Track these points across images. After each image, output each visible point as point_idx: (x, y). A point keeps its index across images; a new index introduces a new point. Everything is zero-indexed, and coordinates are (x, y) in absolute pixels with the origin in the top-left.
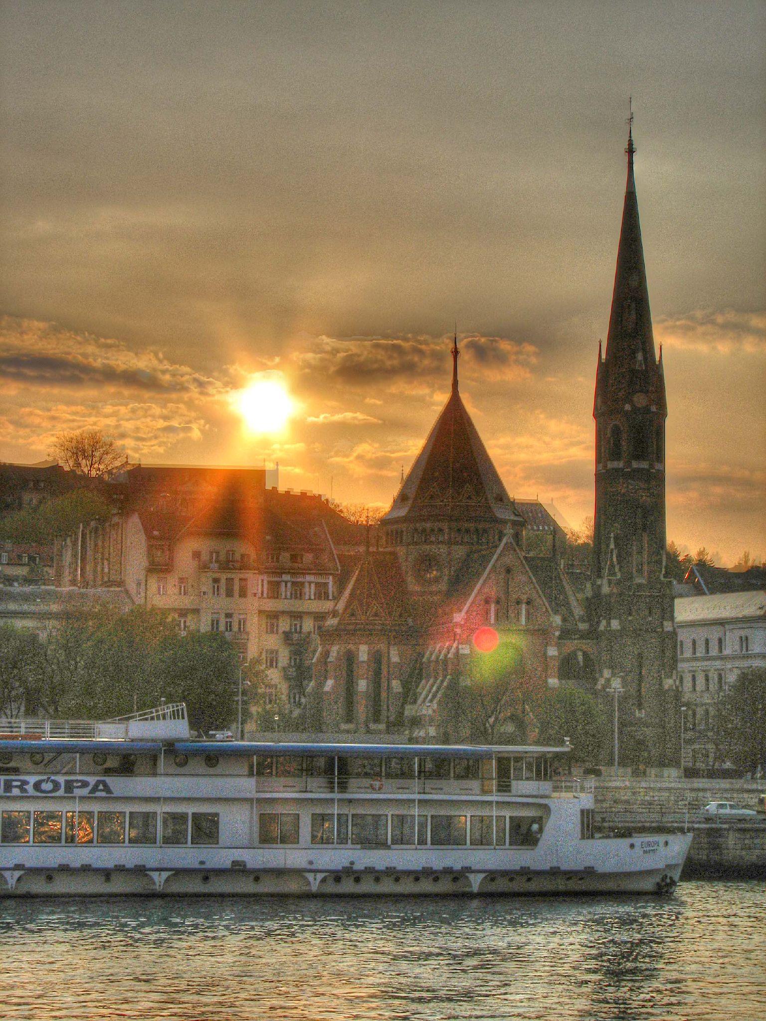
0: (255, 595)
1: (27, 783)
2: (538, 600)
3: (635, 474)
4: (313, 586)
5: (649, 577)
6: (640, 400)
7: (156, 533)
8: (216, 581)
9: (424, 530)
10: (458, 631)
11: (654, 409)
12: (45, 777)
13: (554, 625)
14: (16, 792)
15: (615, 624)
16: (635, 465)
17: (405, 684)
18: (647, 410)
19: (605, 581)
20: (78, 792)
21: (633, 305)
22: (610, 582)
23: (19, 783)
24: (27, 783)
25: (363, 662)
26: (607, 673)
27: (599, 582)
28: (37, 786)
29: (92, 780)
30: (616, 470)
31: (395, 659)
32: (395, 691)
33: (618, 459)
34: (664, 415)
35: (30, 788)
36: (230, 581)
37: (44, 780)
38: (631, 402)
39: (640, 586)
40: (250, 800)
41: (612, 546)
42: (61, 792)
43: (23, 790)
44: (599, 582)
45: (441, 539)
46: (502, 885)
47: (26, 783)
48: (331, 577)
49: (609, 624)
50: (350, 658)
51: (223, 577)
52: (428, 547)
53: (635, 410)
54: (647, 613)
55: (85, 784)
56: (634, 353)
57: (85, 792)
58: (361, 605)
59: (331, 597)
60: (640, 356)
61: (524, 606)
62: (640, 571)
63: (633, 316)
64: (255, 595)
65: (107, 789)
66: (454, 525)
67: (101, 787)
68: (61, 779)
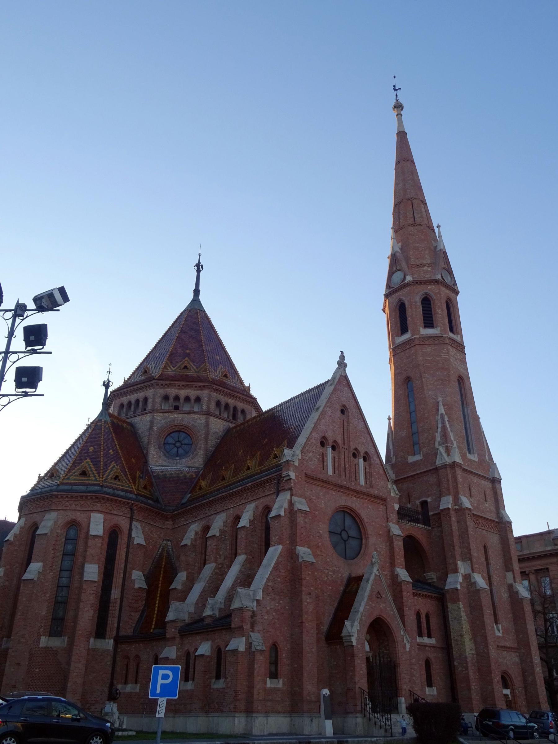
2: (375, 458)
9: (177, 398)
10: (292, 475)
17: (150, 578)
25: (95, 537)
26: (463, 567)
31: (139, 538)
32: (137, 586)
45: (196, 409)
52: (181, 416)
58: (96, 463)
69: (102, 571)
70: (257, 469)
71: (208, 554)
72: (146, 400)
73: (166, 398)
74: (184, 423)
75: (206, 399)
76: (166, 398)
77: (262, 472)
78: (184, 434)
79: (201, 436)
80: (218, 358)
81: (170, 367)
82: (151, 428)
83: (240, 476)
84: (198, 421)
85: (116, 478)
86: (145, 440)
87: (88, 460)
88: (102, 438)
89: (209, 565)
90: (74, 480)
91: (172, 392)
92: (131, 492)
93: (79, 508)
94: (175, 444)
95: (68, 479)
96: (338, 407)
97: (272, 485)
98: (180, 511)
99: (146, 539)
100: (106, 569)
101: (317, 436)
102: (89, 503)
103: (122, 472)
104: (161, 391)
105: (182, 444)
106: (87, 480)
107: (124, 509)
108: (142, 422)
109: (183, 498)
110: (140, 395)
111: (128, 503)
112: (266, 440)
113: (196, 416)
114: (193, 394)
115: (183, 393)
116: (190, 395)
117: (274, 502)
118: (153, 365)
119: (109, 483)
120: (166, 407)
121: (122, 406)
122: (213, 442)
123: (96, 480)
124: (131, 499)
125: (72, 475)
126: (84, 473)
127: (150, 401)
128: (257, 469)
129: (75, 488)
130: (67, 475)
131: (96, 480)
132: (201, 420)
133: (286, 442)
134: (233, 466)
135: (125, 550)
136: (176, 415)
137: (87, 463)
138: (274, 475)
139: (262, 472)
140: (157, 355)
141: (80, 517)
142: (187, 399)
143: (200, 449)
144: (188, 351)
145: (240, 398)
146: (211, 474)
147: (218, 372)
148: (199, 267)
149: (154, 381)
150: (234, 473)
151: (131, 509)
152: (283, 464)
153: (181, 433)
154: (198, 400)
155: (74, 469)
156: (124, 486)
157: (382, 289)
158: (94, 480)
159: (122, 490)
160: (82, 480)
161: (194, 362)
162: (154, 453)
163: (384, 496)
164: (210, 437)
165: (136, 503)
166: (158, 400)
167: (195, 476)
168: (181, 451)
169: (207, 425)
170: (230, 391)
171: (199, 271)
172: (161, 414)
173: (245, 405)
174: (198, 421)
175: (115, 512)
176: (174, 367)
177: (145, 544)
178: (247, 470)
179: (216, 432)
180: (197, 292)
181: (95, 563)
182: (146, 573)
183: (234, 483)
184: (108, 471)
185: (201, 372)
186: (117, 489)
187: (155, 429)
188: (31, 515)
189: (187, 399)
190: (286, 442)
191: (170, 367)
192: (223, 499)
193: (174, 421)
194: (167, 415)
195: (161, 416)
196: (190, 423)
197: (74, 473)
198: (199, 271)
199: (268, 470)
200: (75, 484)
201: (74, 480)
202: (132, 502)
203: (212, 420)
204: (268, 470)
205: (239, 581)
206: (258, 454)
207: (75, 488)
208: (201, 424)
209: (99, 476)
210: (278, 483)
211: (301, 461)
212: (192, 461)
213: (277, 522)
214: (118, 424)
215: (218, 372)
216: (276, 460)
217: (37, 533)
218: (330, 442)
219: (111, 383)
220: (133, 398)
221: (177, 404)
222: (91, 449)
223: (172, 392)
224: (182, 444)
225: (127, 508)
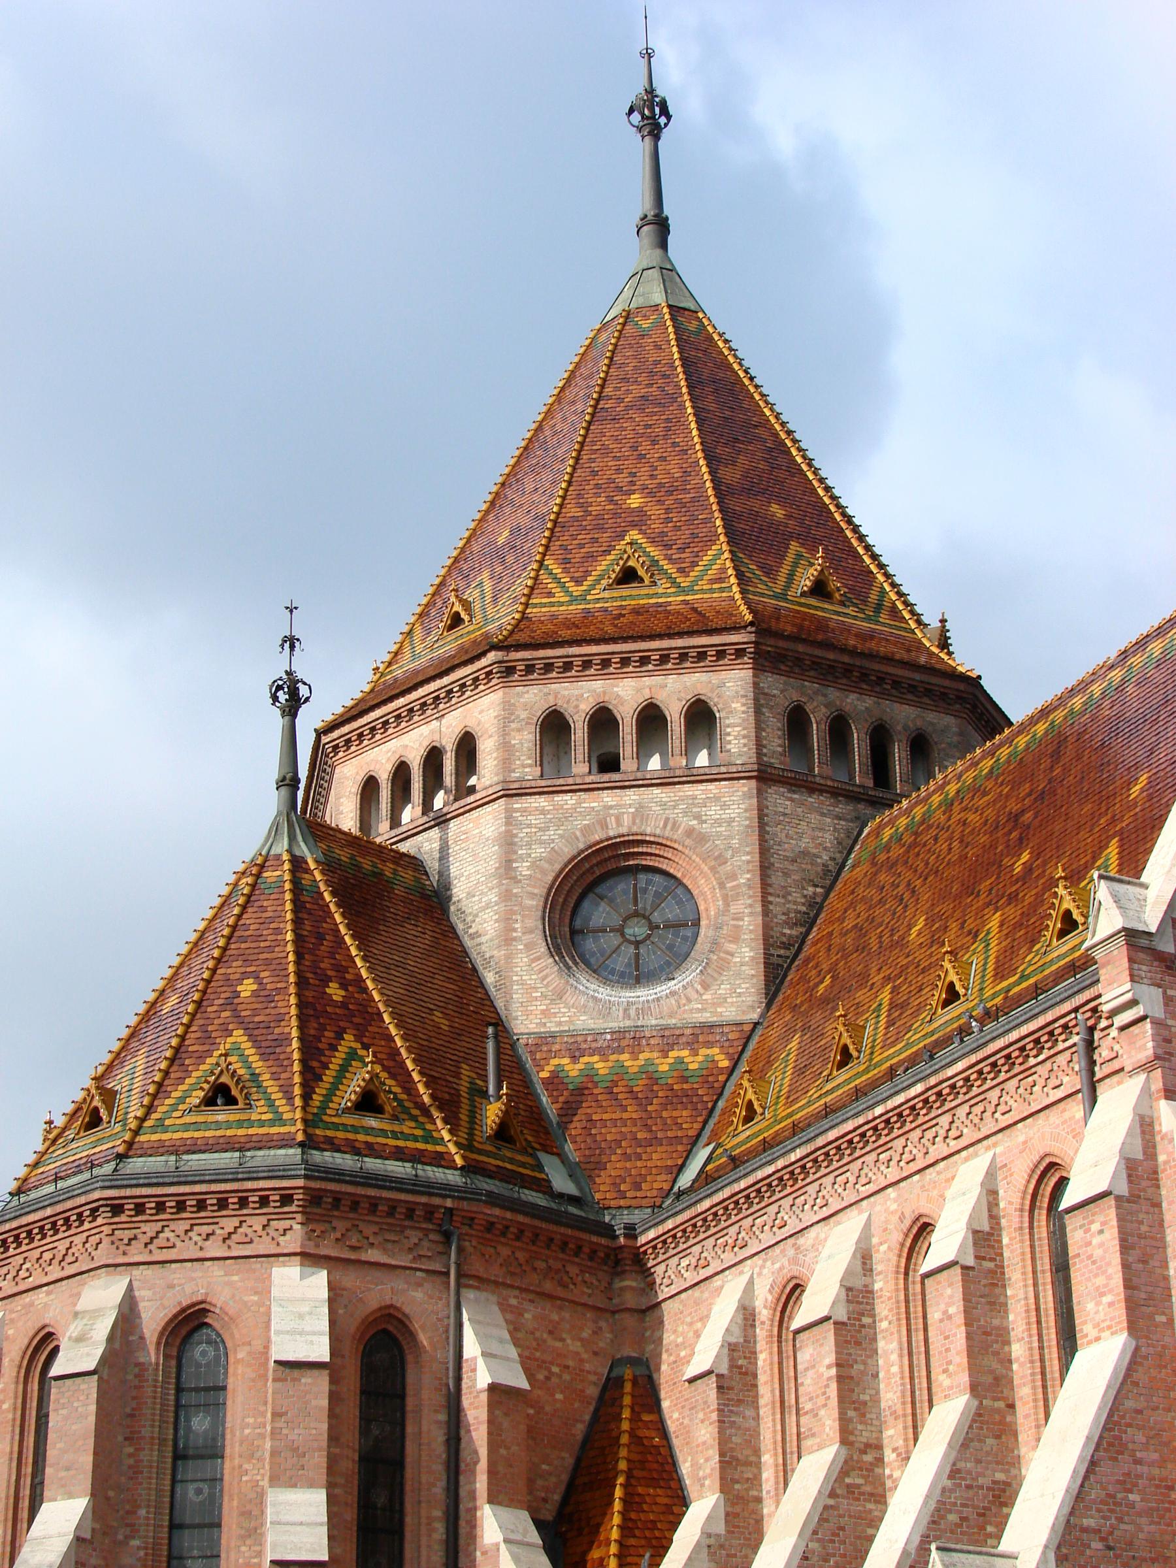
9: (603, 721)
52: (631, 797)
58: (270, 1050)
69: (350, 1515)
70: (988, 993)
71: (806, 1406)
72: (467, 746)
74: (651, 828)
75: (737, 706)
77: (1013, 1002)
78: (657, 878)
79: (733, 877)
80: (777, 511)
81: (563, 586)
83: (917, 1038)
84: (713, 811)
87: (239, 1036)
88: (289, 936)
89: (811, 1457)
90: (186, 1127)
91: (578, 697)
93: (214, 1249)
94: (621, 931)
95: (160, 1126)
97: (1062, 1060)
98: (670, 1224)
99: (529, 1366)
100: (365, 1505)
102: (257, 1223)
103: (392, 1076)
104: (535, 698)
105: (653, 927)
106: (240, 1124)
107: (414, 1236)
109: (681, 1168)
111: (430, 1212)
112: (1025, 857)
113: (698, 790)
114: (673, 690)
115: (626, 693)
116: (661, 699)
117: (1078, 1136)
118: (488, 586)
119: (336, 1127)
121: (370, 786)
123: (279, 1120)
124: (446, 1190)
125: (174, 1108)
127: (487, 750)
128: (988, 993)
129: (195, 1161)
130: (150, 1109)
131: (279, 1120)
132: (724, 806)
133: (1112, 851)
134: (885, 996)
135: (442, 1417)
136: (608, 798)
137: (237, 1048)
138: (1067, 1006)
139: (1013, 1002)
140: (501, 540)
142: (651, 719)
143: (736, 939)
144: (635, 501)
145: (896, 684)
146: (794, 1044)
147: (782, 579)
149: (492, 656)
150: (890, 1023)
152: (1098, 955)
153: (642, 877)
155: (181, 1080)
156: (407, 1137)
158: (272, 1123)
159: (399, 1155)
160: (218, 1125)
161: (668, 547)
162: (531, 979)
164: (777, 880)
165: (465, 1205)
166: (526, 739)
167: (725, 1064)
170: (846, 659)
171: (653, 130)
172: (541, 802)
173: (931, 716)
174: (713, 811)
175: (373, 1255)
176: (578, 582)
177: (524, 1384)
178: (946, 1003)
179: (805, 853)
180: (659, 226)
181: (311, 1485)
182: (548, 1515)
183: (891, 1073)
184: (329, 1077)
185: (703, 584)
186: (372, 1150)
187: (523, 868)
188: (27, 1298)
189: (651, 719)
190: (1112, 851)
191: (563, 586)
192: (848, 1146)
193: (604, 825)
194: (569, 800)
195: (543, 812)
196: (675, 826)
197: (182, 1100)
198: (653, 130)
199: (1037, 990)
200: (194, 1148)
201: (186, 1127)
202: (449, 1203)
204: (1037, 990)
205: (952, 1518)
206: (994, 923)
207: (195, 1161)
208: (730, 821)
209: (290, 1099)
210: (1090, 1046)
212: (707, 997)
213: (1095, 1227)
214: (358, 867)
215: (782, 579)
216: (1071, 940)
217: (55, 1371)
219: (303, 691)
220: (411, 744)
221: (608, 748)
222: (247, 988)
223: (578, 697)
224: (653, 927)
225: (426, 1232)
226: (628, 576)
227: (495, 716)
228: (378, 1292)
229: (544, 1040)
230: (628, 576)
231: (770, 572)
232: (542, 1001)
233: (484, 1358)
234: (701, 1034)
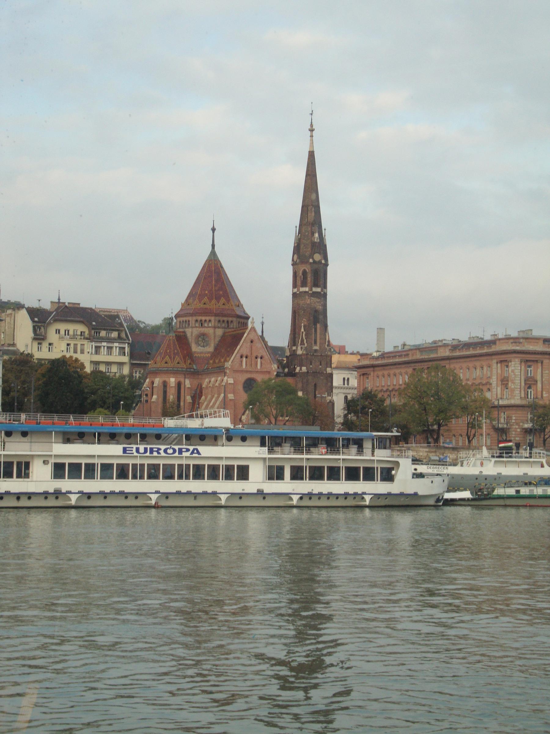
0: (88, 352)
1: (160, 449)
3: (315, 294)
4: (118, 349)
5: (320, 347)
6: (317, 257)
7: (36, 319)
8: (68, 345)
9: (201, 321)
10: (228, 371)
11: (323, 262)
12: (169, 446)
13: (274, 369)
14: (155, 454)
15: (304, 369)
16: (314, 289)
18: (320, 262)
19: (299, 348)
20: (185, 454)
21: (313, 209)
22: (302, 348)
23: (156, 449)
24: (160, 449)
27: (294, 348)
28: (165, 451)
29: (191, 448)
30: (305, 292)
33: (306, 286)
34: (326, 265)
35: (162, 452)
36: (75, 345)
37: (168, 448)
38: (313, 258)
39: (316, 351)
40: (264, 459)
41: (302, 330)
42: (177, 454)
43: (159, 453)
44: (294, 348)
45: (210, 325)
46: (382, 502)
47: (160, 449)
48: (127, 344)
49: (301, 369)
50: (165, 385)
51: (72, 343)
53: (315, 262)
54: (318, 363)
55: (188, 450)
56: (313, 234)
57: (188, 454)
58: (170, 358)
59: (126, 355)
60: (317, 235)
61: (259, 360)
62: (315, 343)
63: (313, 214)
64: (88, 352)
65: (198, 453)
66: (217, 318)
67: (195, 451)
68: (177, 447)
72: (189, 321)
73: (197, 321)
74: (205, 332)
76: (197, 321)
82: (192, 335)
85: (178, 363)
86: (190, 340)
91: (199, 318)
92: (184, 368)
96: (249, 341)
101: (239, 356)
104: (195, 318)
108: (189, 331)
110: (187, 319)
115: (203, 318)
120: (197, 325)
121: (180, 322)
122: (217, 339)
126: (166, 363)
141: (167, 379)
144: (207, 292)
148: (213, 230)
151: (185, 375)
154: (210, 321)
157: (290, 262)
163: (268, 370)
166: (194, 322)
168: (205, 344)
169: (215, 333)
171: (213, 232)
180: (213, 246)
189: (205, 321)
198: (213, 232)
203: (217, 330)
211: (231, 366)
218: (245, 356)
223: (199, 318)
226: (205, 304)
227: (192, 319)
228: (179, 379)
229: (195, 352)
230: (205, 304)
231: (218, 302)
232: (195, 348)
233: (188, 383)
234: (209, 353)
